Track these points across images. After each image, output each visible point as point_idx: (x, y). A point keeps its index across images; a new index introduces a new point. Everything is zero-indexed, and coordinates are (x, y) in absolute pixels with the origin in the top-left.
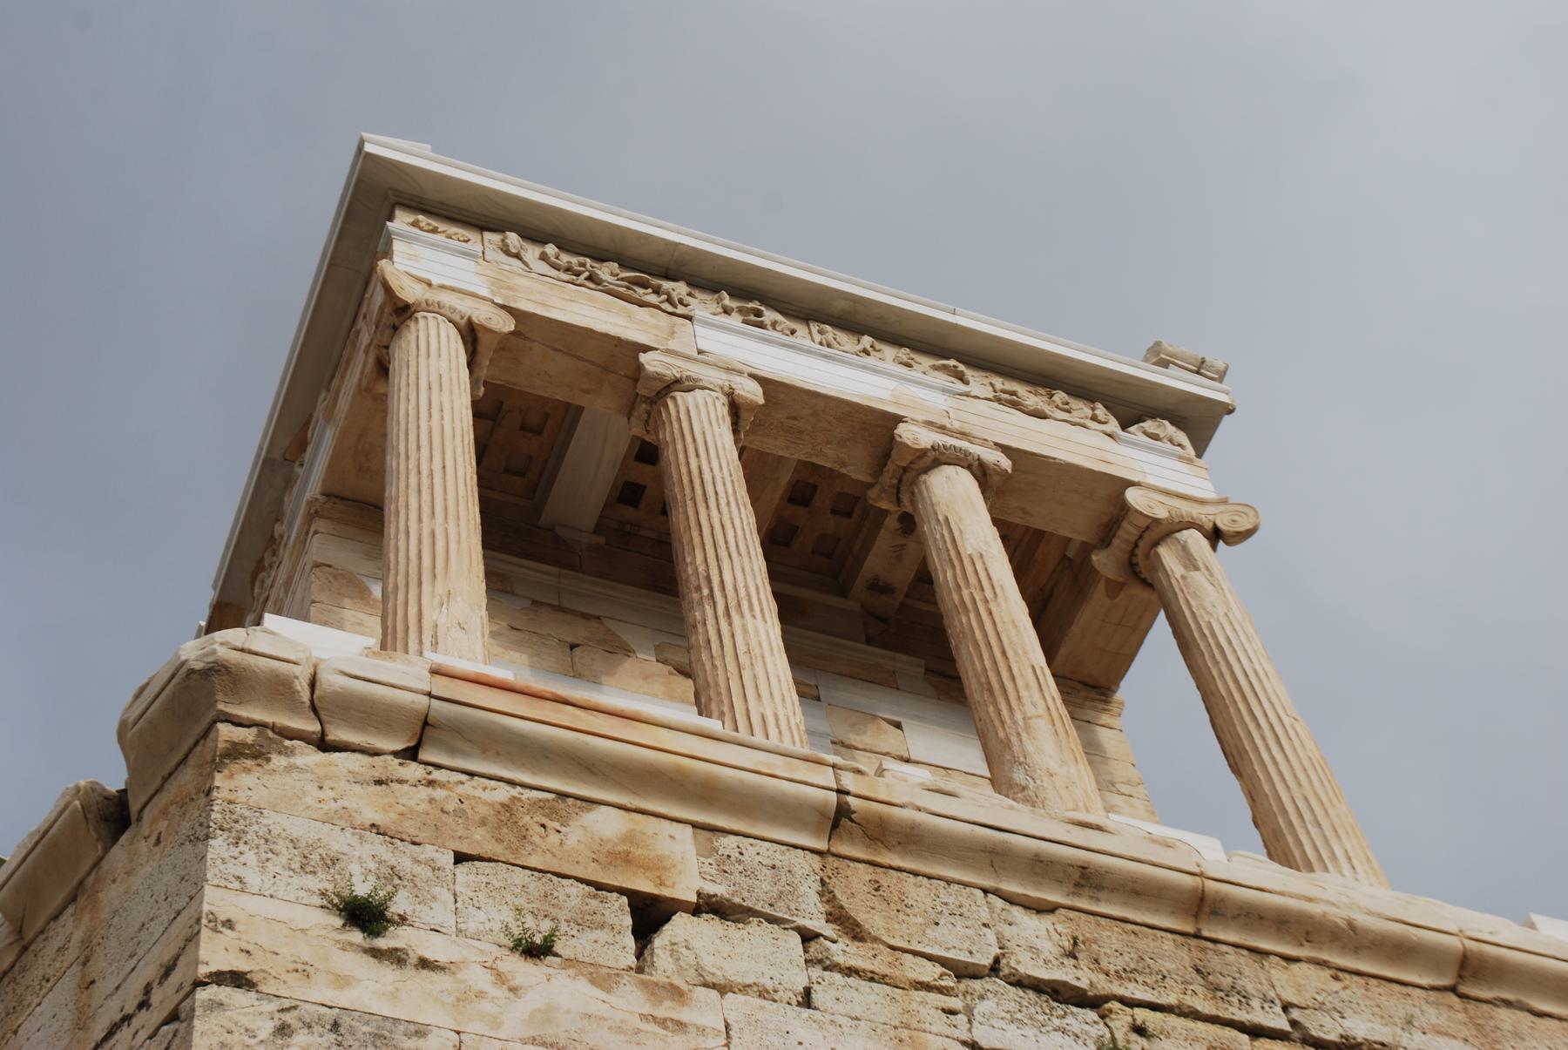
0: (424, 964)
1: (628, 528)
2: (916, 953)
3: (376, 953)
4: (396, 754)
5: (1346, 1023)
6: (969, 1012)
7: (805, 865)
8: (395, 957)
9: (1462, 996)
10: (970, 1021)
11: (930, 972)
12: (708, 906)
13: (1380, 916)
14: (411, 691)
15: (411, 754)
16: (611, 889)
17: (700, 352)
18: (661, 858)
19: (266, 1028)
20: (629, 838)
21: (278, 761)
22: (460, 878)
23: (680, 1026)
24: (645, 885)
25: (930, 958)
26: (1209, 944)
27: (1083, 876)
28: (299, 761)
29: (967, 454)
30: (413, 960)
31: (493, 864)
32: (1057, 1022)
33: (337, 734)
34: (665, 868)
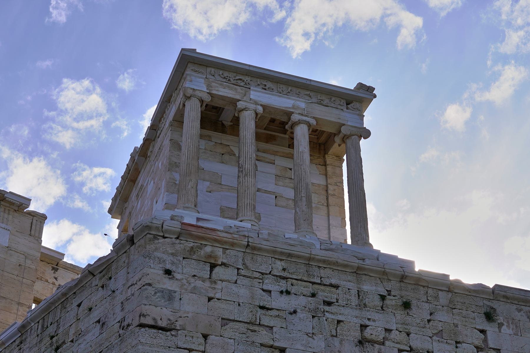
2: (256, 272)
4: (175, 238)
5: (332, 281)
6: (263, 282)
7: (241, 255)
9: (357, 273)
10: (263, 284)
11: (257, 275)
12: (223, 264)
15: (177, 238)
16: (207, 262)
18: (216, 255)
20: (212, 252)
22: (184, 263)
24: (213, 262)
26: (311, 265)
28: (160, 241)
31: (189, 259)
32: (278, 284)
33: (166, 236)
34: (217, 258)
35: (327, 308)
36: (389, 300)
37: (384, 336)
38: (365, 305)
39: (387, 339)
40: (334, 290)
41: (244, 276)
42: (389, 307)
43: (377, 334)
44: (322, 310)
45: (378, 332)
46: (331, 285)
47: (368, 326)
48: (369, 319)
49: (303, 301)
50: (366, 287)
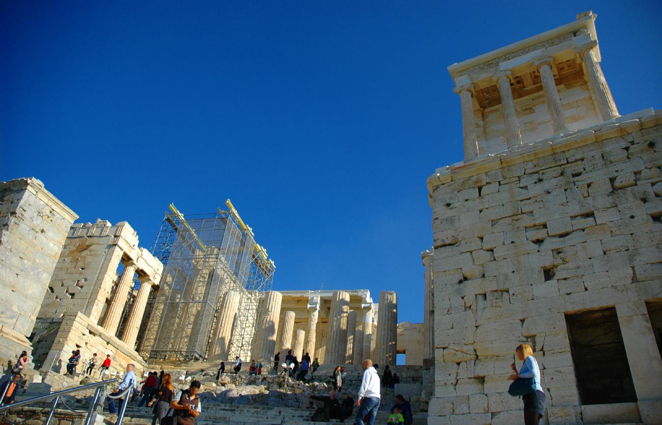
3: (450, 209)
8: (452, 208)
11: (514, 179)
19: (440, 223)
20: (478, 178)
21: (438, 189)
23: (483, 202)
24: (479, 185)
35: (576, 179)
36: (633, 149)
37: (634, 178)
38: (611, 162)
39: (639, 180)
40: (580, 162)
41: (505, 184)
44: (572, 181)
46: (576, 161)
47: (617, 177)
48: (617, 171)
49: (554, 182)
50: (607, 149)
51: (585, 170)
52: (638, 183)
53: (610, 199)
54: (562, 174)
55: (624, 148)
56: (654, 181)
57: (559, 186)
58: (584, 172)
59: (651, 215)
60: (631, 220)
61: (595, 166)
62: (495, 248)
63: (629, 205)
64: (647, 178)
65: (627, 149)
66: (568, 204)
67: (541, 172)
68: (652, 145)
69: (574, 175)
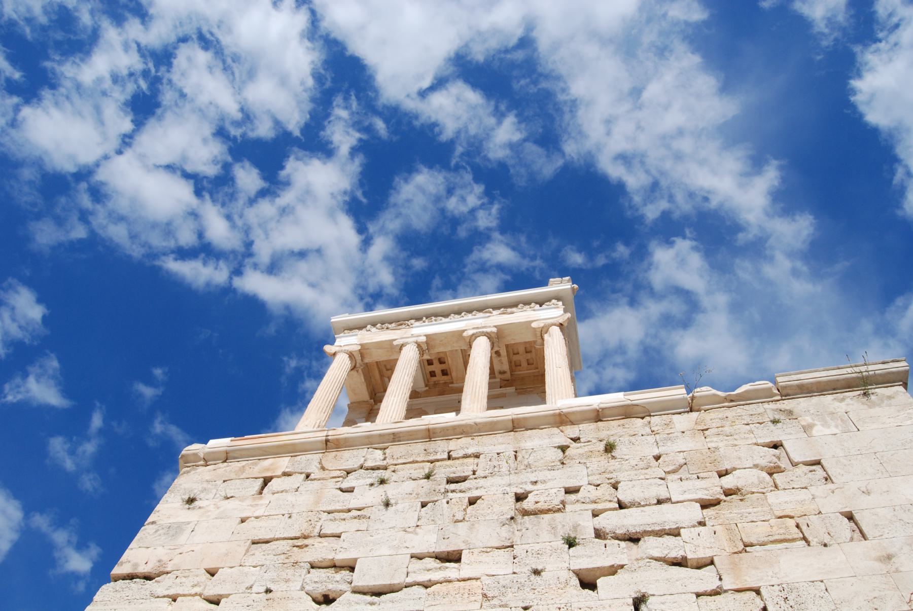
0: (200, 508)
1: (436, 382)
4: (222, 462)
13: (485, 418)
14: (223, 447)
17: (412, 335)
20: (272, 465)
25: (340, 470)
27: (394, 436)
29: (483, 332)
30: (198, 507)
35: (453, 486)
36: (574, 450)
37: (562, 498)
38: (528, 466)
42: (574, 458)
43: (549, 499)
44: (443, 490)
45: (551, 495)
46: (466, 456)
49: (409, 486)
51: (474, 474)
52: (568, 507)
53: (504, 532)
54: (428, 477)
55: (559, 447)
56: (600, 506)
57: (414, 495)
58: (471, 477)
59: (577, 573)
60: (533, 577)
61: (496, 469)
62: (227, 596)
63: (537, 547)
64: (588, 500)
65: (563, 449)
66: (418, 530)
67: (392, 468)
68: (609, 448)
69: (450, 481)
